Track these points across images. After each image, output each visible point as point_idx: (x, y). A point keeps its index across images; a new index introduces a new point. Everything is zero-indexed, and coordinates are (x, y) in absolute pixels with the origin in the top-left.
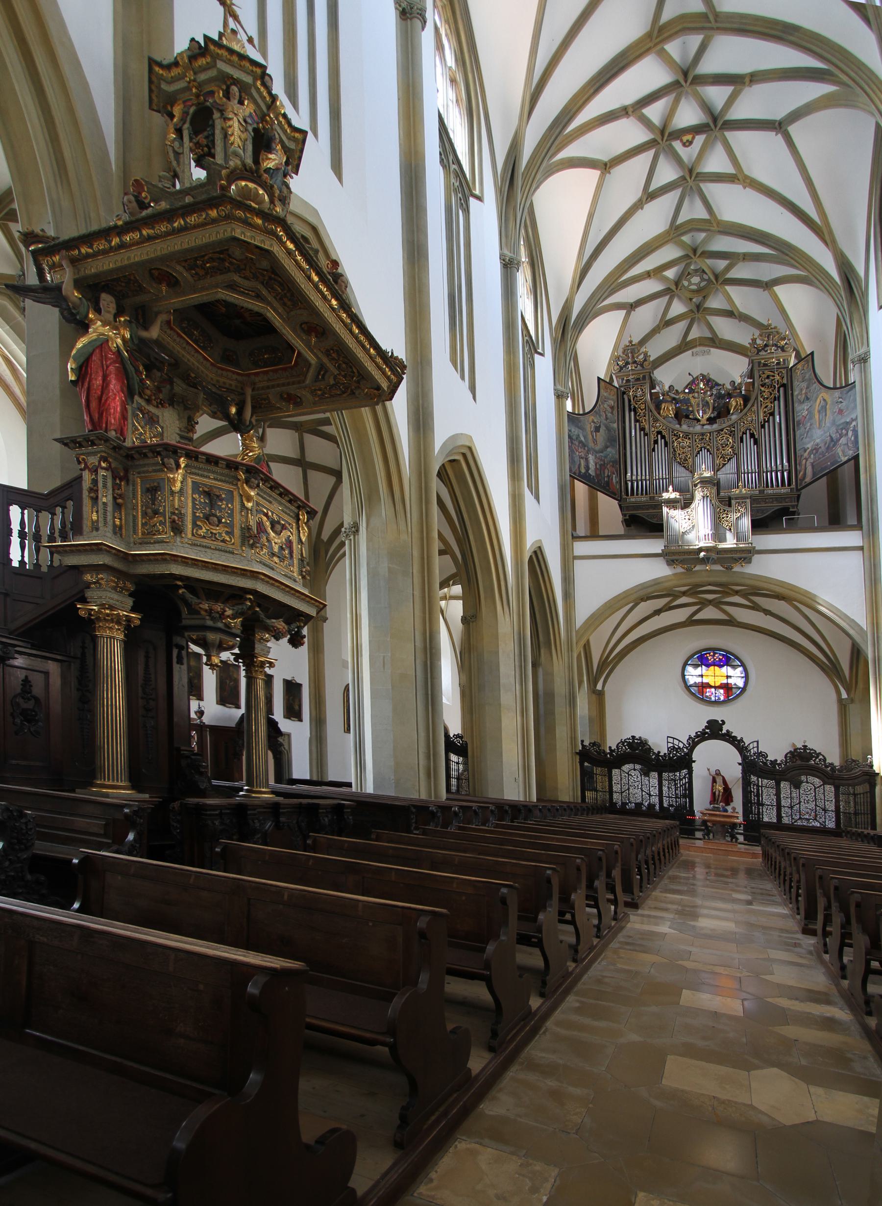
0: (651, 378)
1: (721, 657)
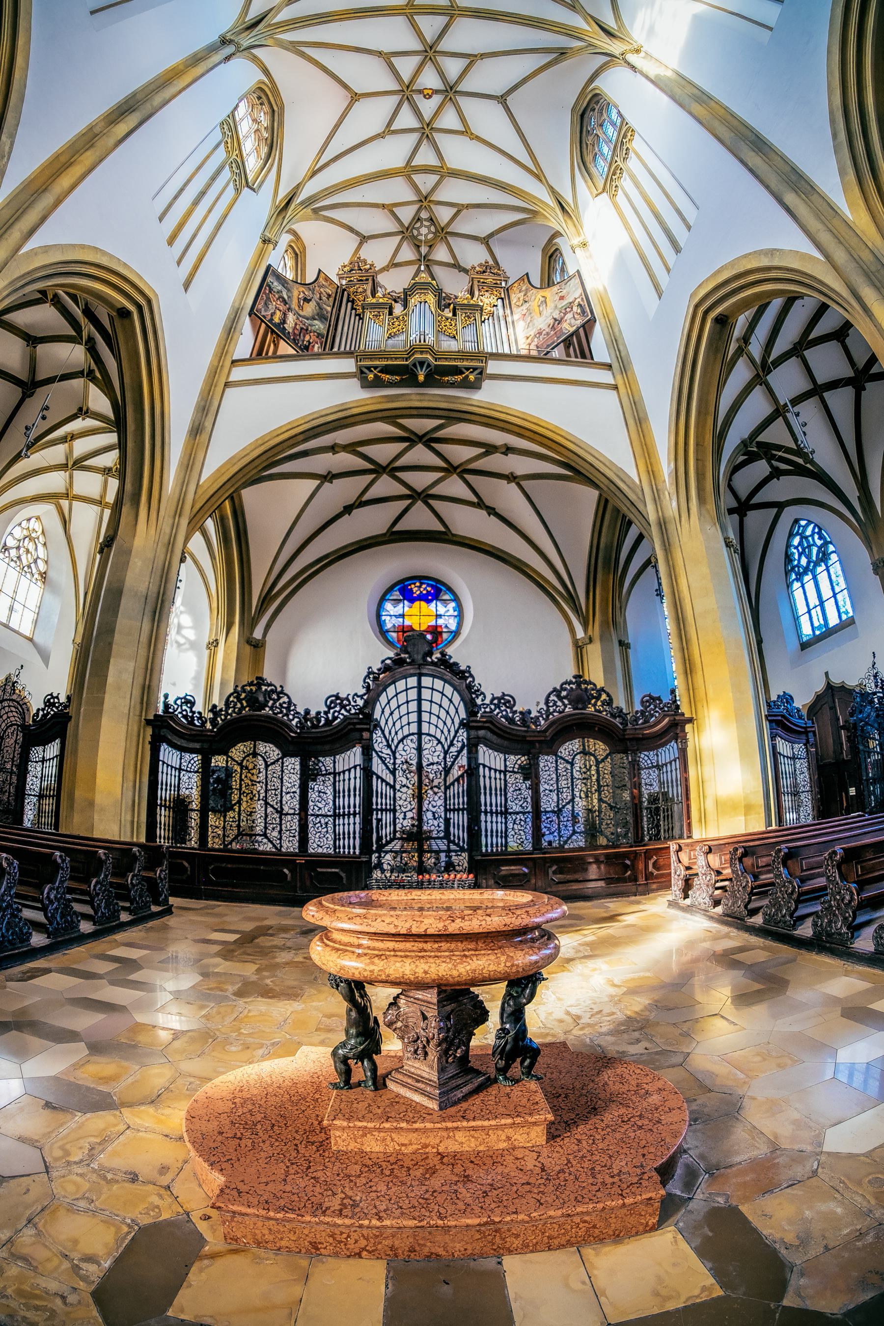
0: (373, 280)
1: (429, 589)
